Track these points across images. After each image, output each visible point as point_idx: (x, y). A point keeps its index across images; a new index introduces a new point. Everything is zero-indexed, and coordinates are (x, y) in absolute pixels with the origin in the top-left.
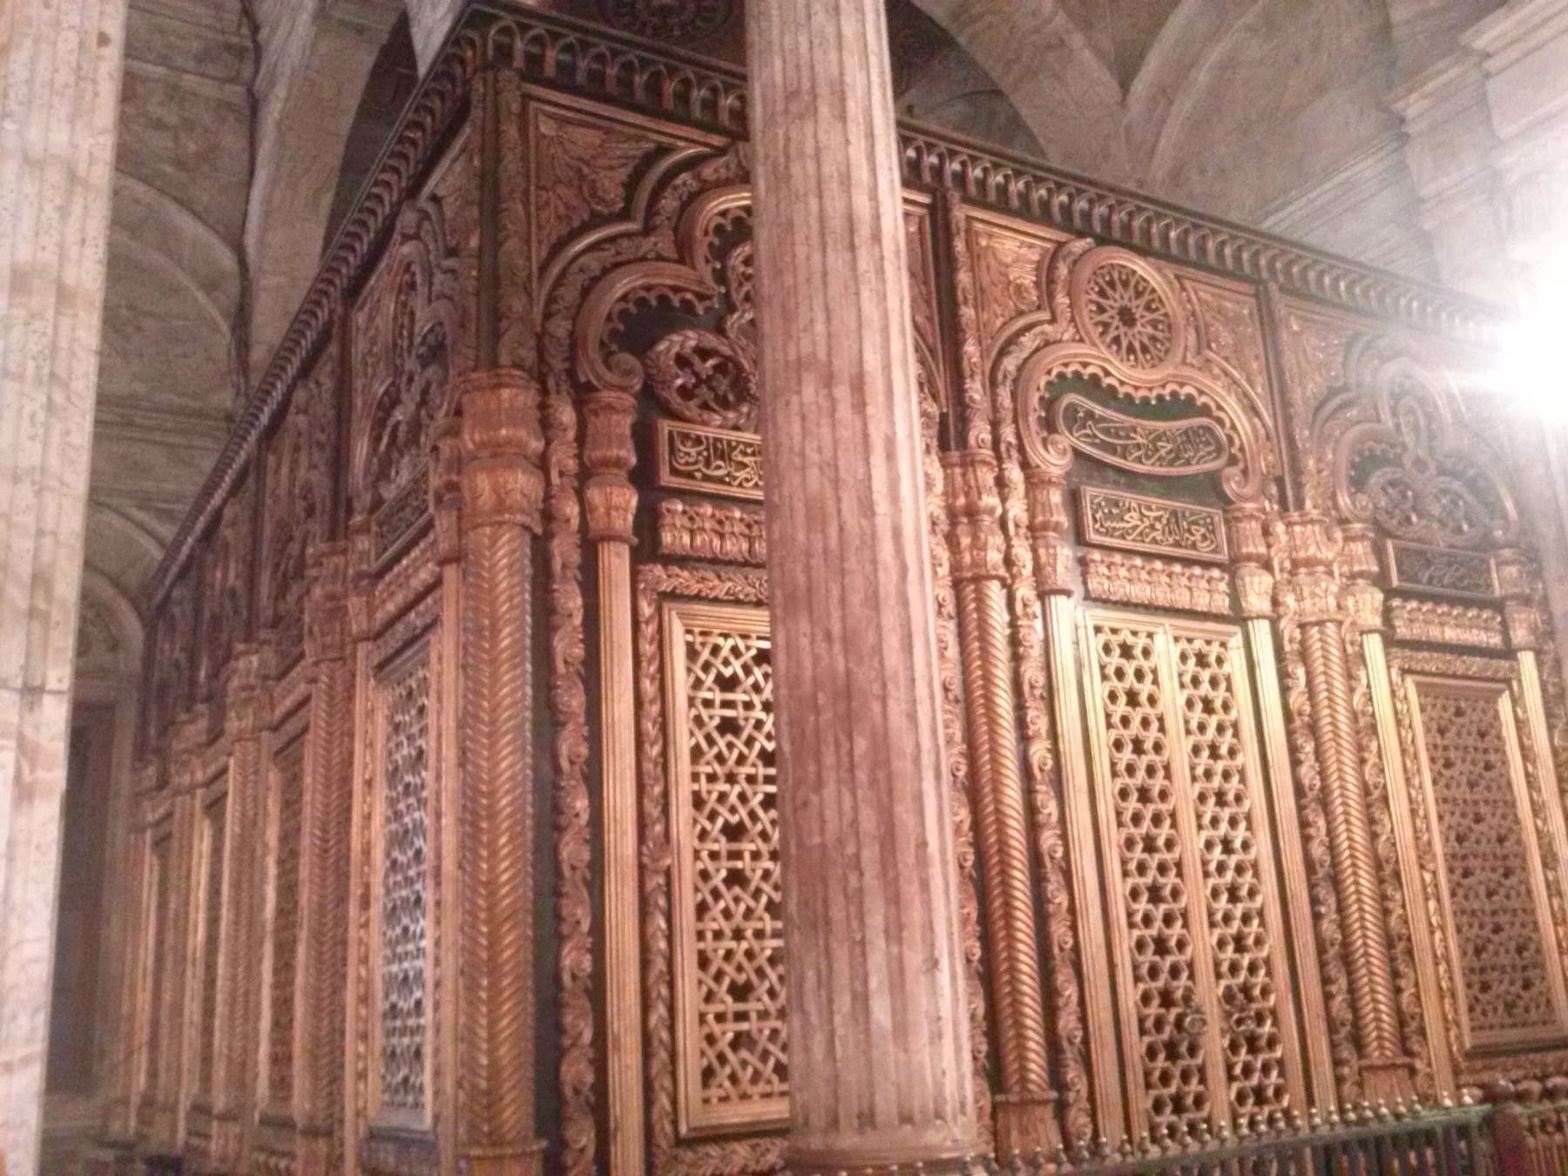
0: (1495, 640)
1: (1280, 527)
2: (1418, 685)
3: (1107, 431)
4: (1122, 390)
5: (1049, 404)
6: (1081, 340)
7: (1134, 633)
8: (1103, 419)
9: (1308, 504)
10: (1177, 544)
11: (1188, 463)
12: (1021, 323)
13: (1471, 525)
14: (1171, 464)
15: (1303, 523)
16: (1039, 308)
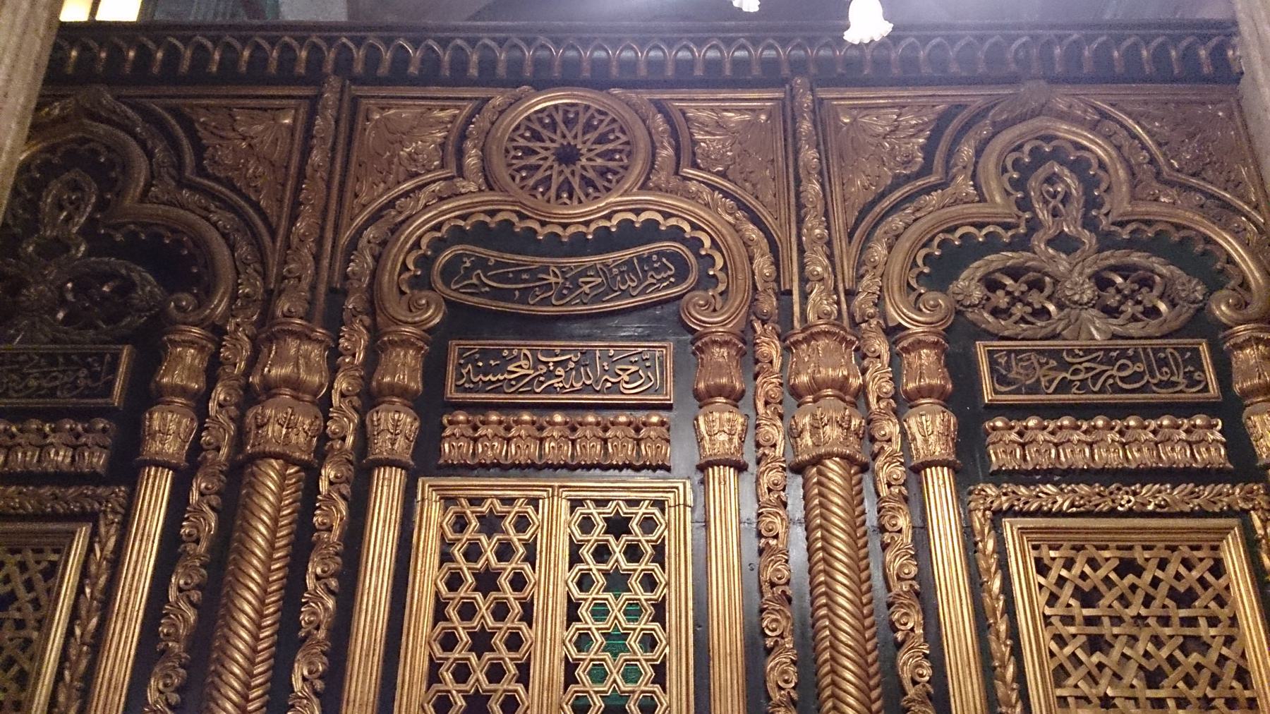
0: (1214, 454)
1: (771, 348)
2: (1023, 531)
3: (502, 278)
4: (542, 232)
5: (425, 262)
6: (491, 189)
7: (509, 501)
8: (499, 265)
9: (811, 317)
10: (586, 388)
11: (625, 294)
12: (407, 186)
13: (1172, 304)
14: (598, 298)
15: (806, 340)
16: (442, 167)
